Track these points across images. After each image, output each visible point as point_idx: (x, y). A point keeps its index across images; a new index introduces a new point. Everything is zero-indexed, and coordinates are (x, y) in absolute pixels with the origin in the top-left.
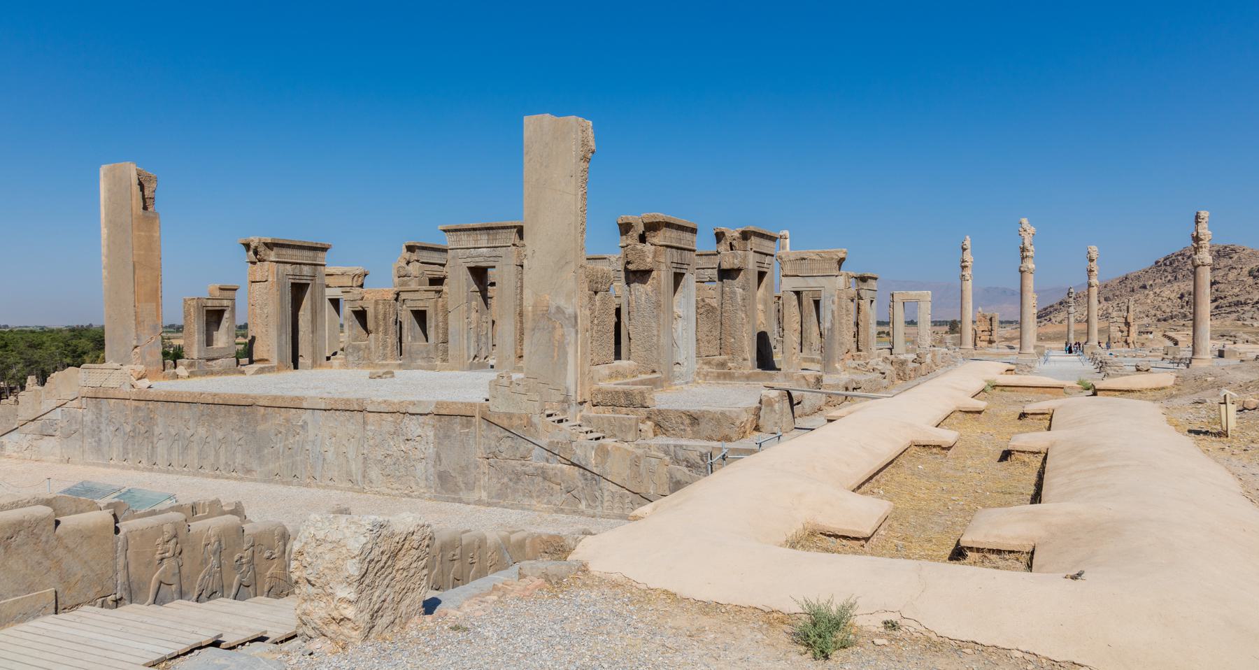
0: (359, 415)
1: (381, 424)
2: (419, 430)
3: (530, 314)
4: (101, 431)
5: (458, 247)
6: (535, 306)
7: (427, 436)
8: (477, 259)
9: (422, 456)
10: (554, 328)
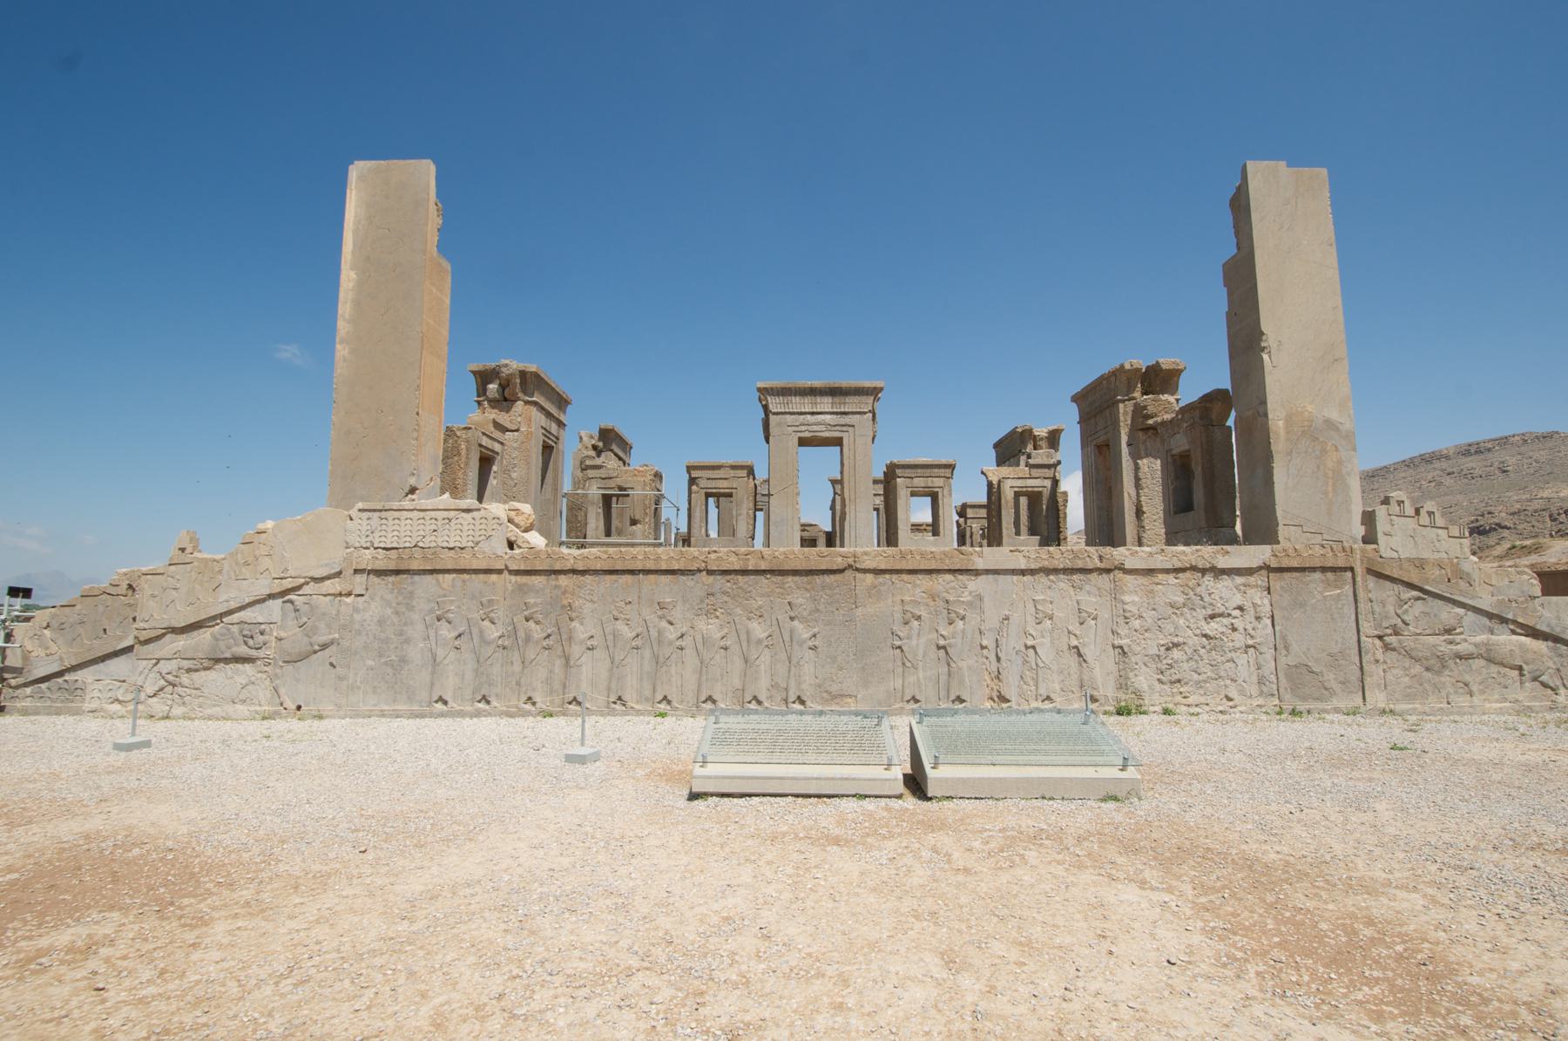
0: (1103, 581)
1: (1152, 591)
2: (1239, 596)
3: (1282, 433)
4: (407, 641)
6: (1289, 420)
7: (1255, 605)
9: (1250, 642)
10: (1324, 451)
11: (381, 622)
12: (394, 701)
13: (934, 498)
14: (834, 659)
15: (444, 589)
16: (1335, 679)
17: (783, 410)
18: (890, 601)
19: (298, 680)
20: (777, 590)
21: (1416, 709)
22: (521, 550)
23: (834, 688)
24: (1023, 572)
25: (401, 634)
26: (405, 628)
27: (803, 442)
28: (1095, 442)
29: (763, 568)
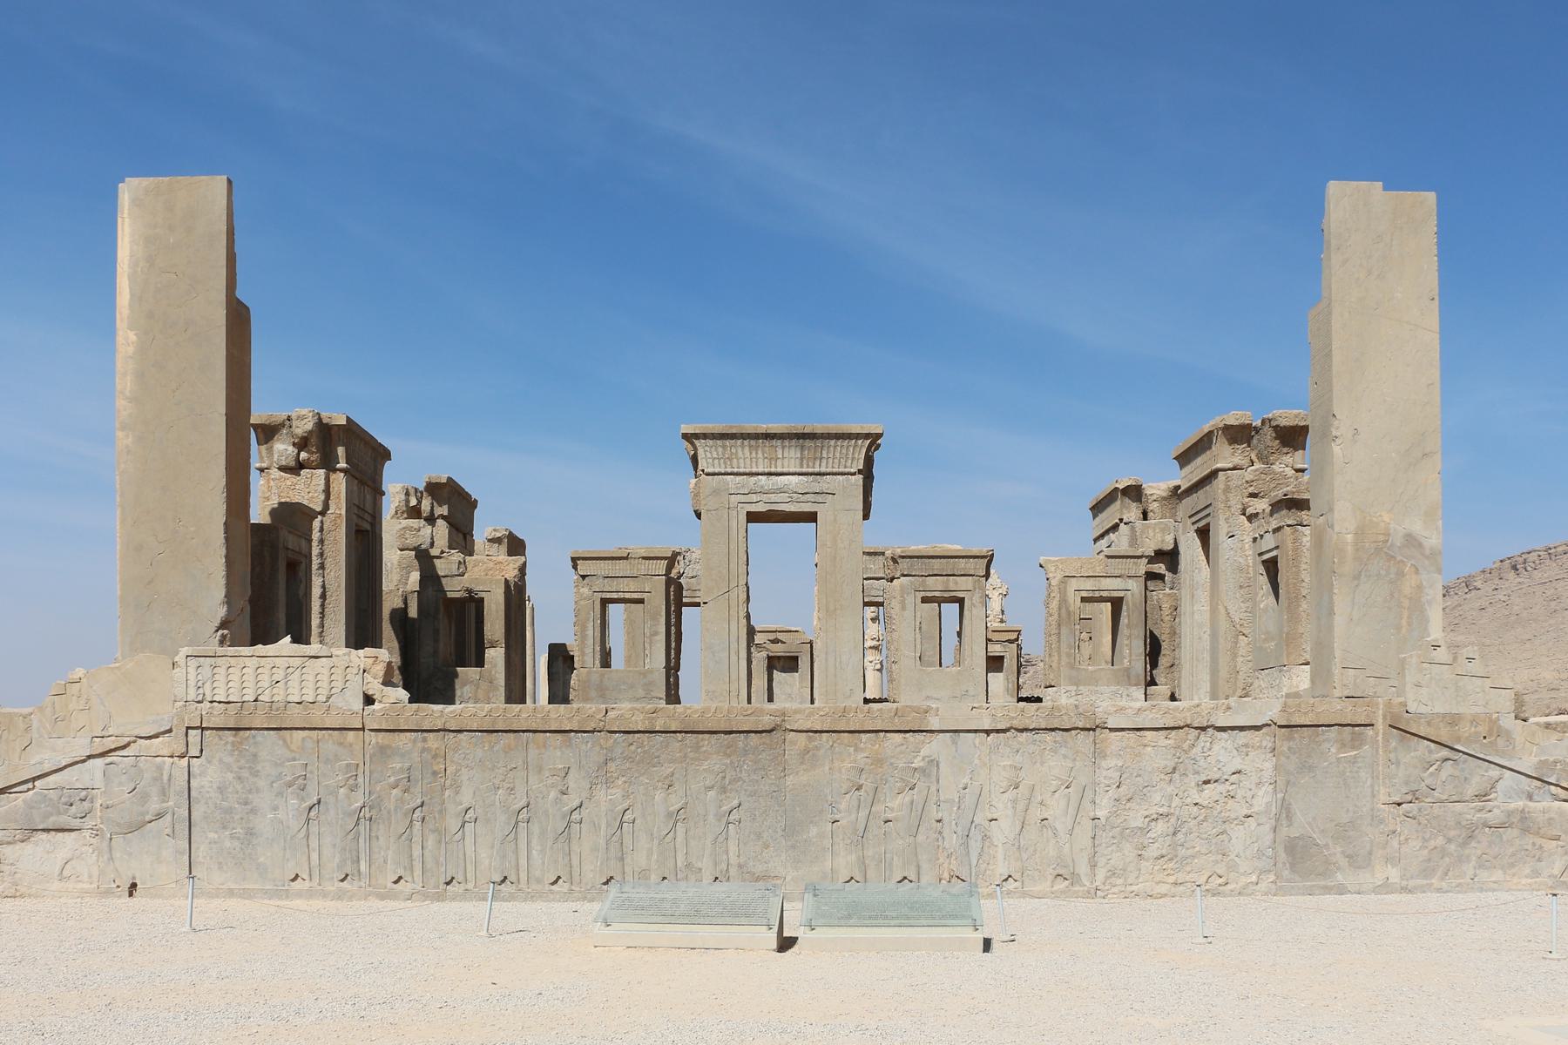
2: (1238, 760)
4: (253, 811)
5: (729, 470)
8: (773, 498)
11: (221, 790)
12: (244, 880)
13: (961, 601)
14: (759, 836)
15: (292, 751)
16: (1343, 852)
17: (723, 471)
18: (827, 768)
19: (130, 854)
20: (692, 755)
21: (1432, 884)
22: (383, 705)
23: (759, 869)
24: (988, 732)
25: (246, 804)
26: (250, 796)
27: (753, 517)
28: (1195, 527)
29: (674, 729)
